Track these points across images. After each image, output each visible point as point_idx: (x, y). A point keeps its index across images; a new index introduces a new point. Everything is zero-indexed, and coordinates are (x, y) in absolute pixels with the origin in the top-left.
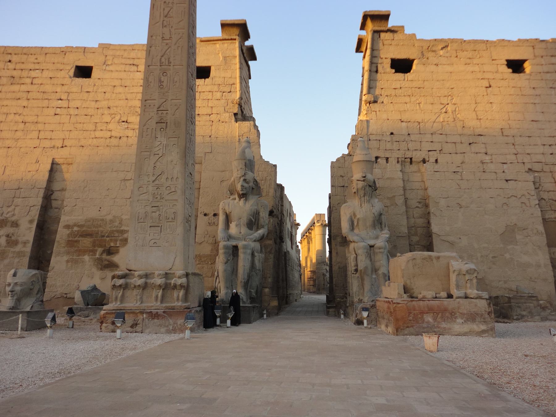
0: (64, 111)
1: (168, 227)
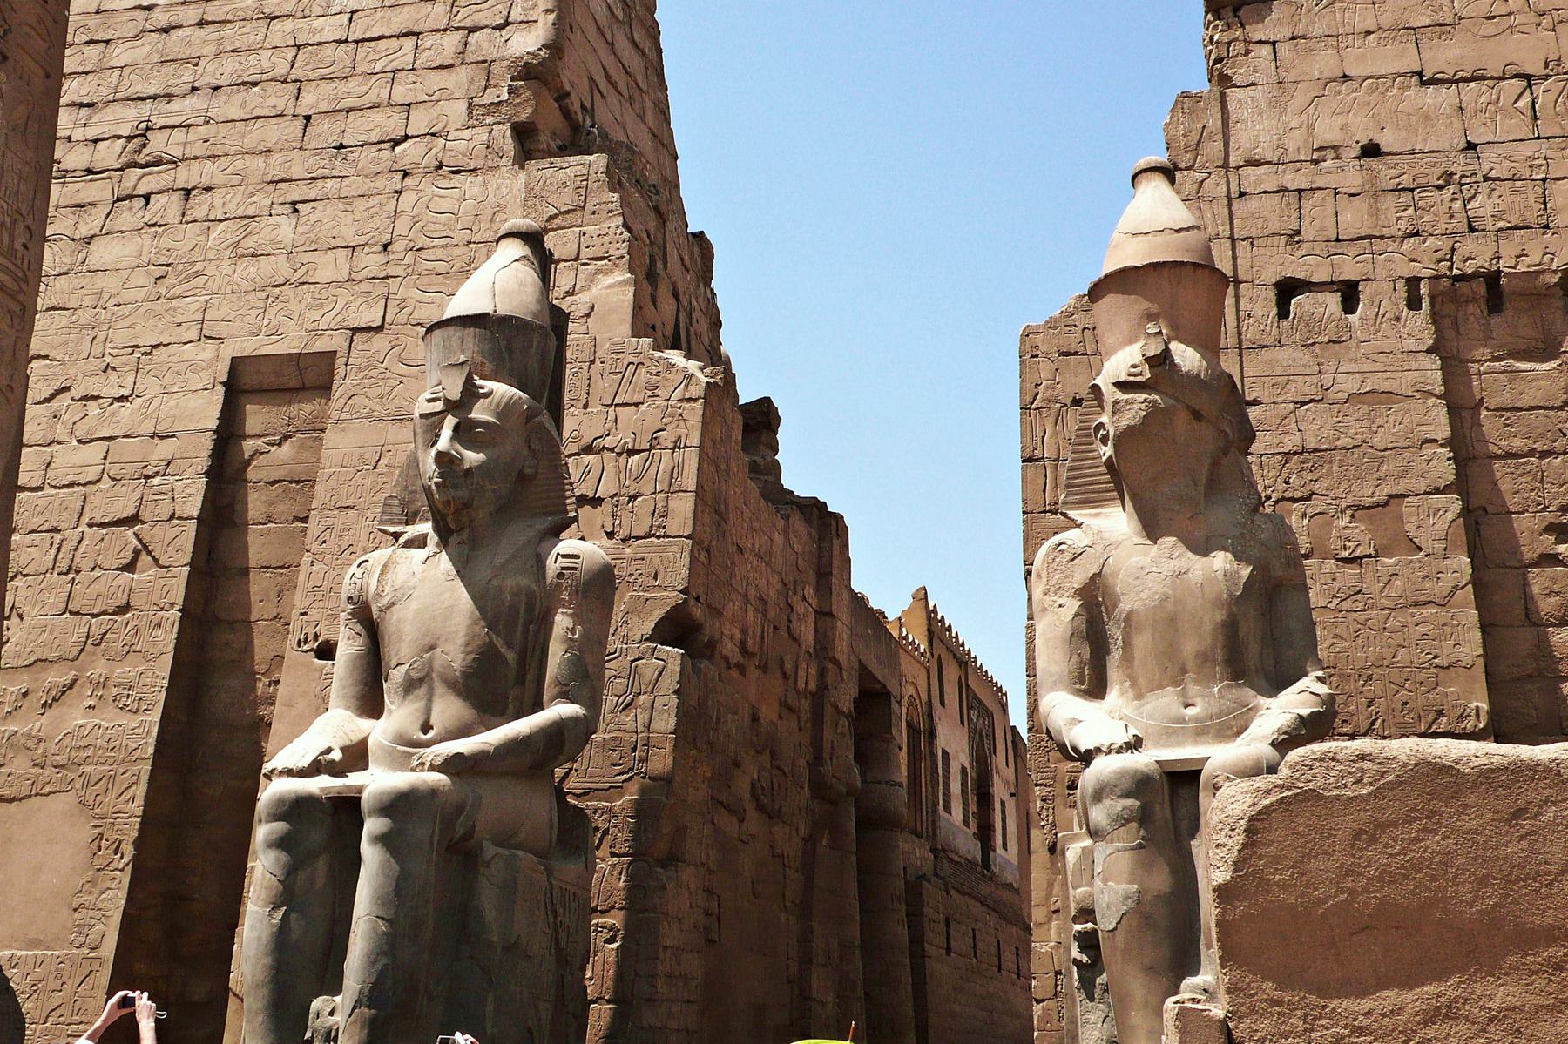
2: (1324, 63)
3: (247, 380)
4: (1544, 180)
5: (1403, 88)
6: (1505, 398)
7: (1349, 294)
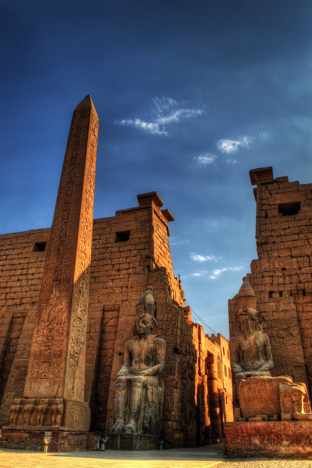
0: (24, 277)
1: (55, 362)
3: (106, 309)
7: (281, 293)
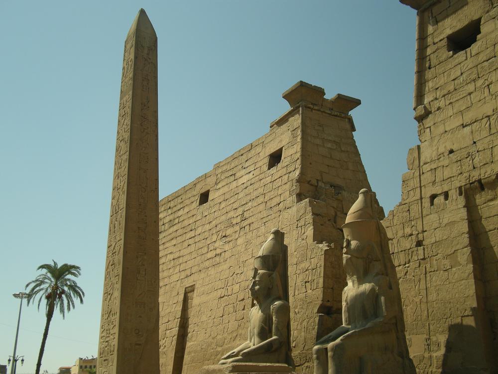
2: (441, 129)
4: (492, 148)
5: (459, 130)
6: (487, 215)
7: (446, 195)
